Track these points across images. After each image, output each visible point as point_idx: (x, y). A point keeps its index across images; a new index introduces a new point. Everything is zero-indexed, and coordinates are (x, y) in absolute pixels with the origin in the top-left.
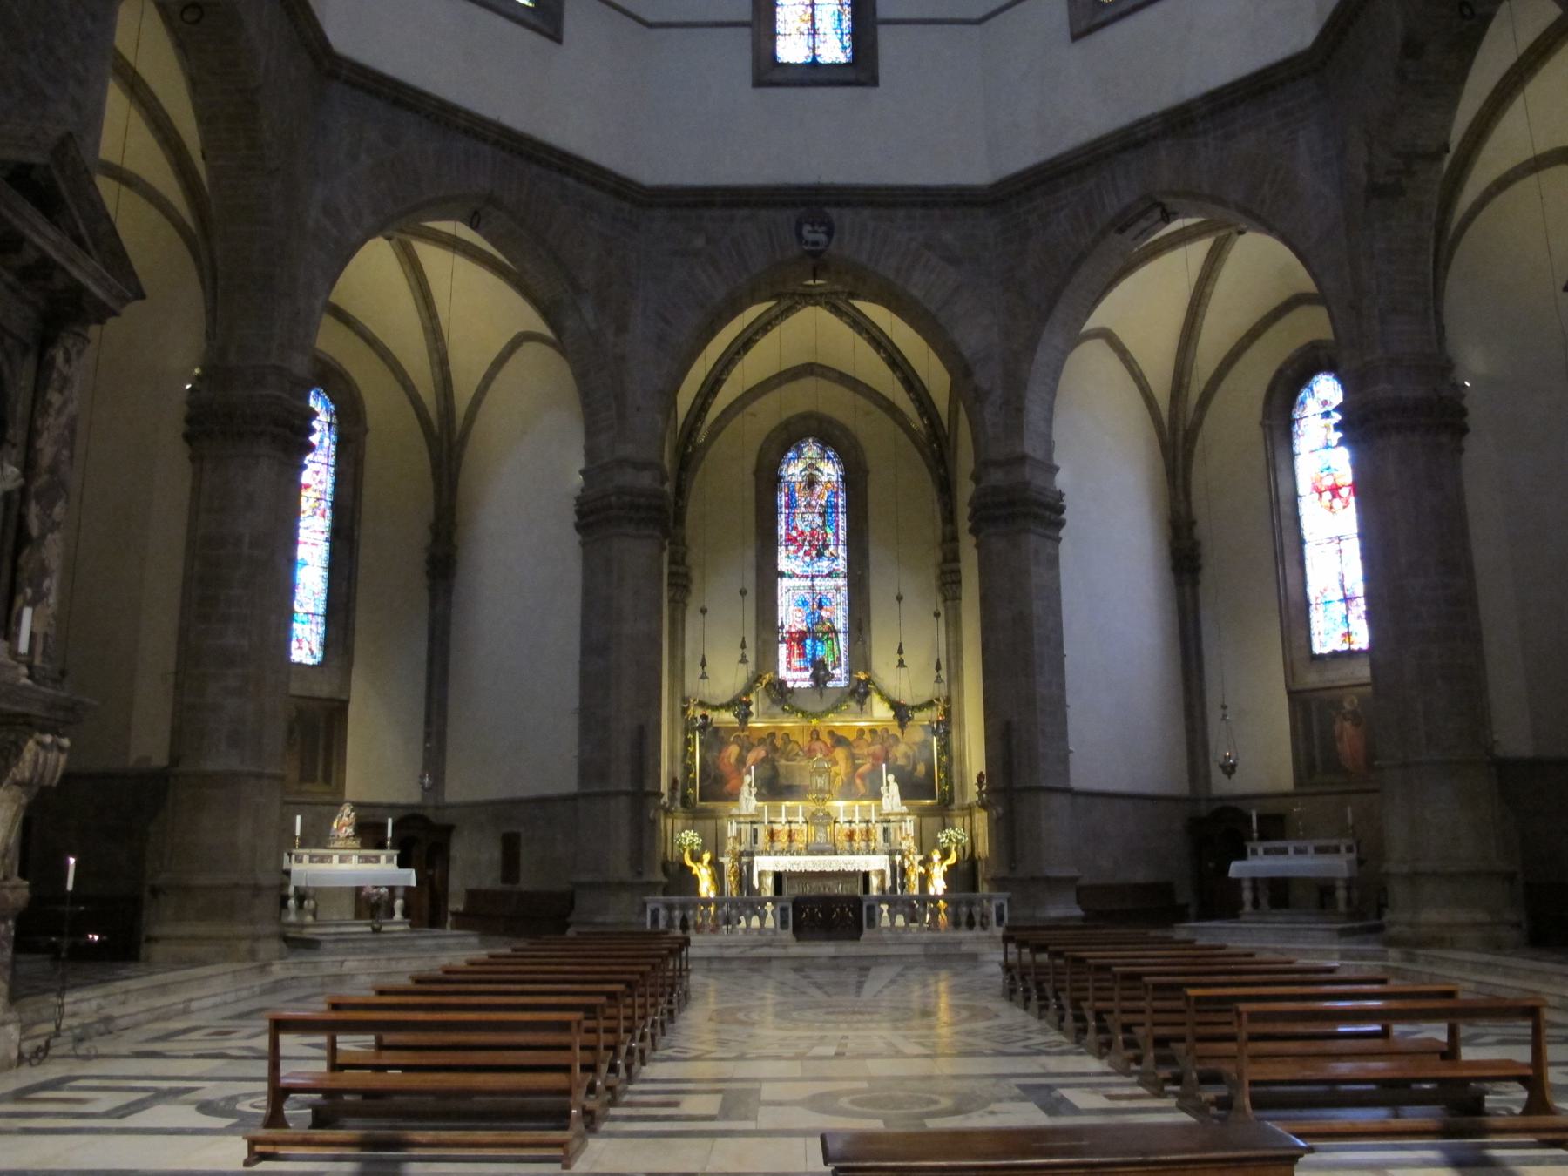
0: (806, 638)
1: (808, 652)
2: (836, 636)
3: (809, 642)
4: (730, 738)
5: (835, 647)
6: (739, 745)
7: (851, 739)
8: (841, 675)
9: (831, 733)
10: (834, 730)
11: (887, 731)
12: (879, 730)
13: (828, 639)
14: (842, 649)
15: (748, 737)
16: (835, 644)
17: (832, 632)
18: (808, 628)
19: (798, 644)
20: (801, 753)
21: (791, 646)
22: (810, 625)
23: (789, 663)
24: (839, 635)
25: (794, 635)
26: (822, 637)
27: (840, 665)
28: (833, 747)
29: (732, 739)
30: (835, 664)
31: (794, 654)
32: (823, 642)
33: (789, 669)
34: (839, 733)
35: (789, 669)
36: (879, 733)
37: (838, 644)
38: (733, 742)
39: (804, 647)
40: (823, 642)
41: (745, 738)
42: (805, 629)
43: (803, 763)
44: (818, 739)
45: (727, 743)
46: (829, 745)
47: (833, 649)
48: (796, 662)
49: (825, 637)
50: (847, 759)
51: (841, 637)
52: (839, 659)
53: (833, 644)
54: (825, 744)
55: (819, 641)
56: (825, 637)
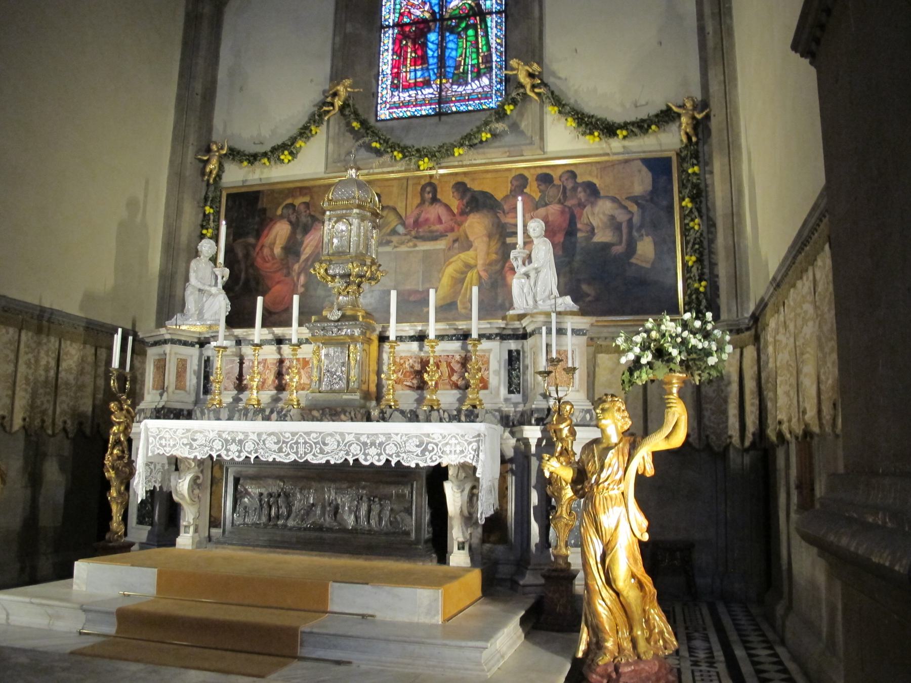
0: (429, 31)
1: (430, 53)
2: (483, 21)
3: (433, 37)
4: (276, 209)
5: (481, 41)
6: (291, 222)
7: (499, 195)
8: (491, 86)
9: (461, 188)
10: (467, 180)
11: (573, 175)
12: (556, 175)
13: (466, 29)
14: (493, 42)
15: (307, 205)
16: (480, 33)
17: (475, 15)
18: (433, 13)
19: (414, 43)
20: (401, 229)
21: (401, 48)
22: (436, 9)
23: (396, 76)
24: (489, 19)
25: (407, 29)
26: (458, 26)
27: (490, 69)
28: (464, 213)
29: (279, 212)
30: (479, 70)
31: (405, 59)
32: (459, 34)
33: (395, 87)
34: (475, 186)
35: (395, 87)
36: (557, 182)
37: (486, 35)
38: (282, 217)
39: (424, 46)
40: (459, 34)
41: (302, 208)
42: (427, 15)
43: (404, 248)
44: (435, 200)
45: (271, 220)
46: (455, 211)
47: (477, 42)
48: (411, 74)
49: (463, 25)
50: (490, 236)
51: (491, 21)
52: (488, 59)
53: (476, 36)
54: (448, 207)
55: (452, 33)
56: (463, 25)
